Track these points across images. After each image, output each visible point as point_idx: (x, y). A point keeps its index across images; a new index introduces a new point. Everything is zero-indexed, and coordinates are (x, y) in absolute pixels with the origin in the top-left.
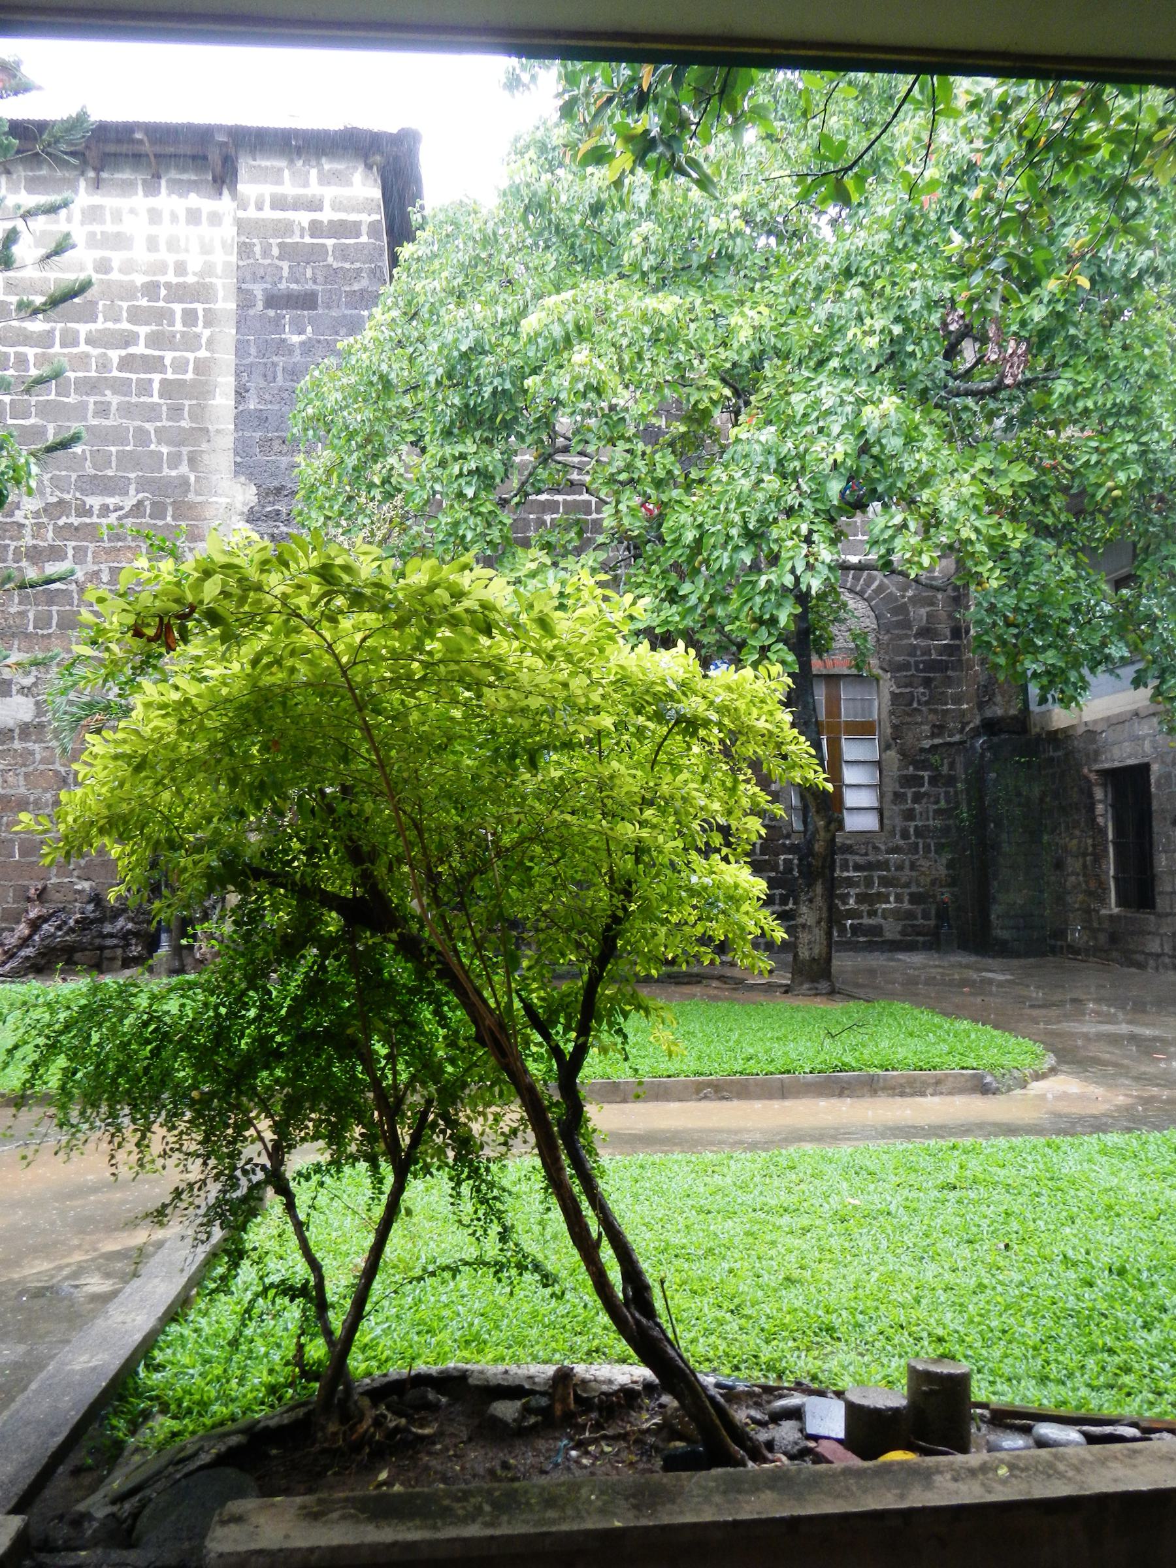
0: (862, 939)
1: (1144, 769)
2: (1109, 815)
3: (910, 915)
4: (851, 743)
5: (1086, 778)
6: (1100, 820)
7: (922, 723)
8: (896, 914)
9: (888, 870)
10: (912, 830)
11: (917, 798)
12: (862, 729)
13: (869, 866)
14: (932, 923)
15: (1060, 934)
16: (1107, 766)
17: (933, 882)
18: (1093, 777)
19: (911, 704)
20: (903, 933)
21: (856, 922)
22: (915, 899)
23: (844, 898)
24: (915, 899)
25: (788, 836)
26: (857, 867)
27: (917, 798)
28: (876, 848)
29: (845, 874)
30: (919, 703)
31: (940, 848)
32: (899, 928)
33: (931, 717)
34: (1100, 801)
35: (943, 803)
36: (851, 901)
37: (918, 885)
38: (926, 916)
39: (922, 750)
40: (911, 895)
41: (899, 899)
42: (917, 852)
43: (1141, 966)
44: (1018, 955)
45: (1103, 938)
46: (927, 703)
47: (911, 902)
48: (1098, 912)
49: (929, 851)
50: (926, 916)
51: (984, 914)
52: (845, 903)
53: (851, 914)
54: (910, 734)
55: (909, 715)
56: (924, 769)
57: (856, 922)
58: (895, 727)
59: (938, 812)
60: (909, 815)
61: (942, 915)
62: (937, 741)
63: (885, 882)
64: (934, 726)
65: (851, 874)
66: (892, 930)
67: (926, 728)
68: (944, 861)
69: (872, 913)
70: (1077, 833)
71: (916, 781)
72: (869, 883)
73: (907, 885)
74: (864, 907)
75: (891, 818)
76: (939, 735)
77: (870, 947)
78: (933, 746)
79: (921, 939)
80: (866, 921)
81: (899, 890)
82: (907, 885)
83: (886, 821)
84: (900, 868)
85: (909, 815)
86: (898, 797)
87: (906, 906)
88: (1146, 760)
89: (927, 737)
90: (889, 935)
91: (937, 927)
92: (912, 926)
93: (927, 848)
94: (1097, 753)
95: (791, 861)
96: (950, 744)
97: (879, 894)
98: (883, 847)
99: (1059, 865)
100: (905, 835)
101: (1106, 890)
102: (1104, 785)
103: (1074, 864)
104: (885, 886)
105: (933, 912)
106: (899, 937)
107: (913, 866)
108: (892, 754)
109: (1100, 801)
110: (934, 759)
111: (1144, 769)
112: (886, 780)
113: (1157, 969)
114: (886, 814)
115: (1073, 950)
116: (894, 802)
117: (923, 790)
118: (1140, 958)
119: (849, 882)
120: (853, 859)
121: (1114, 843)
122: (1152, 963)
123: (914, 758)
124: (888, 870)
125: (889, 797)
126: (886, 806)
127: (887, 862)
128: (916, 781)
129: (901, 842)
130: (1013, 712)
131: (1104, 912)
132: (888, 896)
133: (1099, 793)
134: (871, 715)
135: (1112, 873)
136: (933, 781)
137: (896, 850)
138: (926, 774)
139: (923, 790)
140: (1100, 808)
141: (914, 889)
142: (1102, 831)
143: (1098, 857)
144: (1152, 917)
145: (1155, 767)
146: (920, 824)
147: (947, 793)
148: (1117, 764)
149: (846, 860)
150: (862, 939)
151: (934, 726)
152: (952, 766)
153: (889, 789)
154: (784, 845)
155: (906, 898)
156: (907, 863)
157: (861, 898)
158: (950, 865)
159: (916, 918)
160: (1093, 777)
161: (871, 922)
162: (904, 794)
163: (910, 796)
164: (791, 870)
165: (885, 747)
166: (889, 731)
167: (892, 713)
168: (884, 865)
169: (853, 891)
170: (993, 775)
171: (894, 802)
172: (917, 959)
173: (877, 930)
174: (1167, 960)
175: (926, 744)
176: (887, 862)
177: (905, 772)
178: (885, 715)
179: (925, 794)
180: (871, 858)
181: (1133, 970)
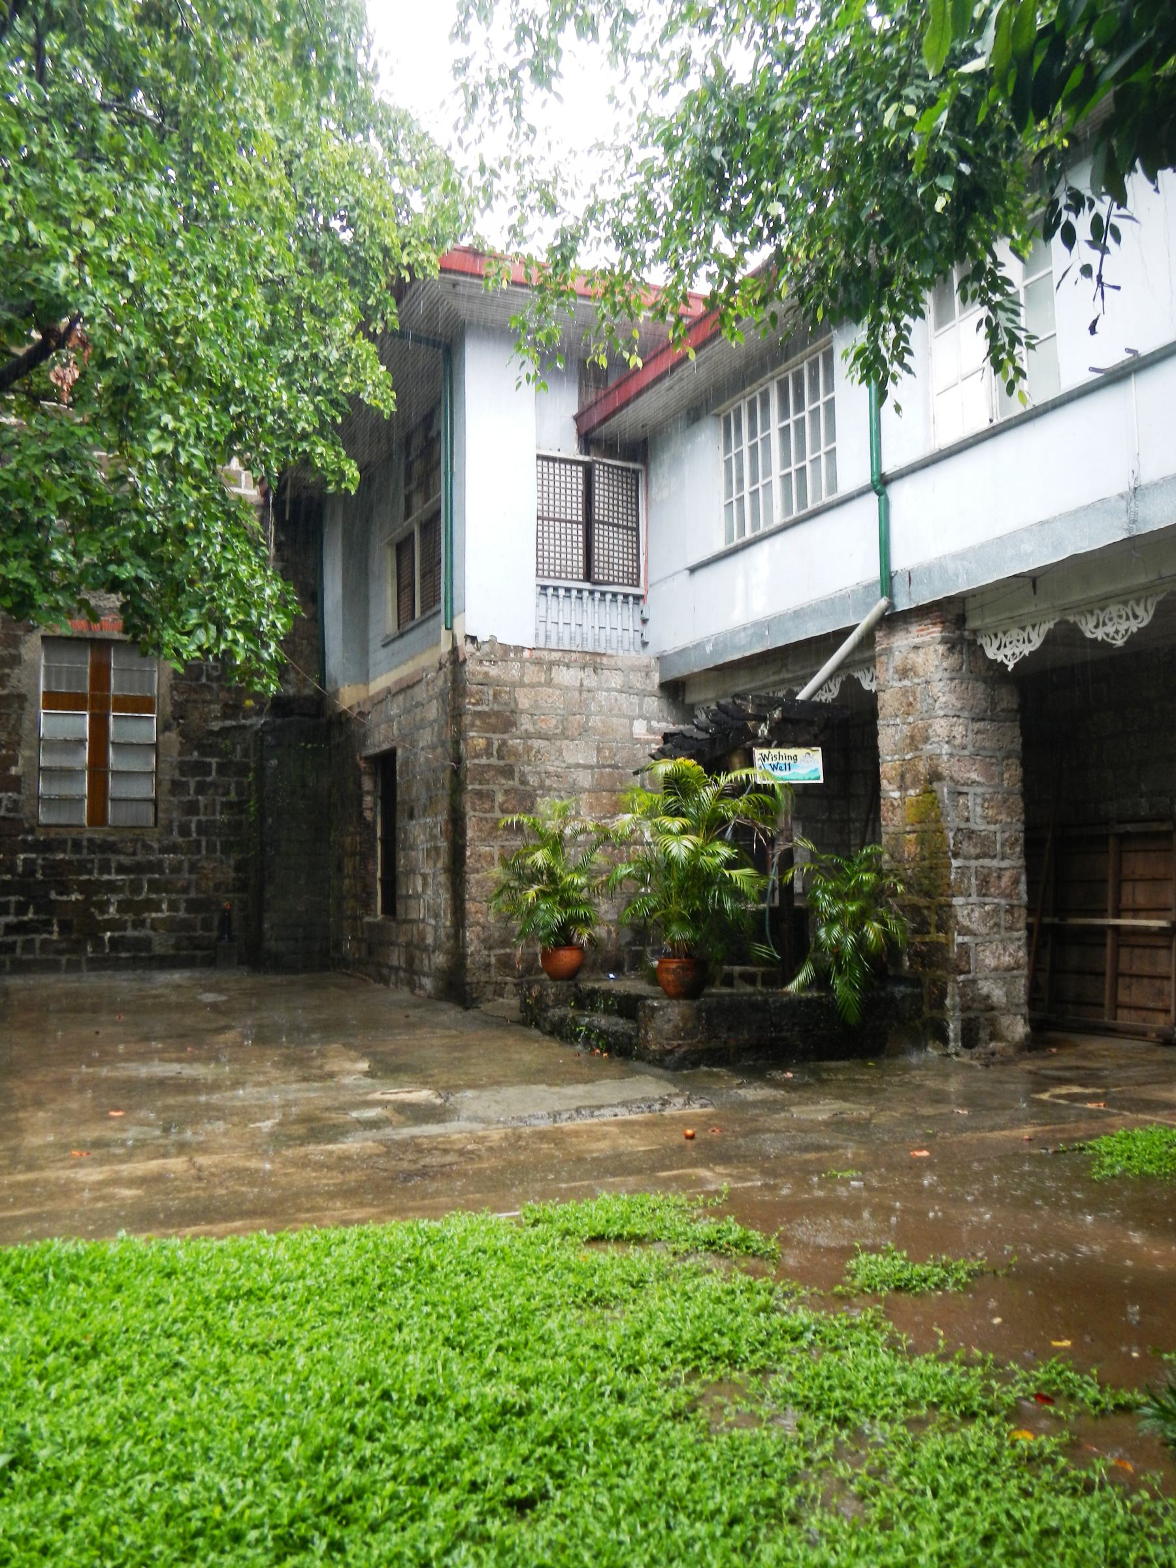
0: (124, 955)
1: (390, 755)
2: (379, 809)
3: (186, 925)
4: (123, 723)
5: (358, 766)
6: (368, 815)
7: (210, 702)
8: (171, 925)
9: (162, 872)
10: (193, 826)
11: (201, 788)
12: (140, 705)
13: (139, 868)
14: (215, 934)
15: (338, 946)
16: (371, 751)
17: (217, 887)
18: (362, 764)
19: (198, 678)
20: (177, 947)
21: (117, 934)
22: (193, 906)
23: (103, 906)
24: (193, 906)
25: (31, 831)
26: (121, 869)
27: (201, 788)
28: (147, 848)
29: (106, 877)
30: (209, 678)
31: (227, 848)
32: (172, 941)
33: (223, 695)
34: (368, 793)
35: (233, 796)
36: (112, 910)
37: (198, 890)
38: (206, 926)
39: (211, 733)
40: (187, 901)
41: (173, 907)
42: (199, 852)
43: (385, 980)
44: (292, 969)
45: (364, 946)
46: (218, 679)
47: (187, 910)
48: (356, 918)
49: (215, 851)
50: (206, 926)
51: (260, 924)
52: (103, 911)
53: (111, 925)
54: (196, 714)
55: (196, 692)
56: (213, 755)
57: (117, 934)
58: (175, 704)
59: (228, 806)
60: (191, 808)
61: (226, 922)
62: (229, 723)
63: (155, 886)
64: (226, 705)
65: (113, 877)
66: (161, 944)
67: (216, 708)
68: (232, 862)
69: (139, 924)
70: (352, 829)
71: (201, 768)
72: (136, 888)
73: (185, 890)
74: (128, 917)
75: (167, 811)
76: (234, 716)
77: (132, 964)
78: (223, 729)
79: (199, 953)
80: (130, 933)
81: (174, 896)
82: (185, 890)
83: (160, 815)
84: (176, 869)
85: (191, 808)
86: (177, 787)
87: (182, 914)
88: (394, 744)
89: (216, 718)
90: (158, 950)
91: (219, 938)
92: (189, 938)
93: (211, 848)
94: (365, 736)
95: (33, 861)
96: (244, 727)
97: (148, 901)
98: (156, 846)
99: (340, 868)
100: (184, 831)
101: (371, 895)
102: (373, 775)
103: (349, 866)
104: (158, 891)
105: (216, 923)
106: (171, 952)
107: (193, 868)
108: (173, 736)
109: (368, 793)
110: (225, 744)
111: (390, 755)
112: (162, 766)
113: (396, 984)
114: (162, 806)
115: (342, 964)
116: (172, 792)
117: (209, 779)
118: (385, 971)
119: (111, 887)
120: (114, 859)
121: (382, 841)
122: (393, 978)
123: (195, 740)
124: (162, 872)
125: (166, 786)
126: (161, 797)
127: (160, 863)
128: (201, 768)
129: (180, 840)
130: (307, 692)
131: (367, 919)
132: (160, 902)
133: (367, 784)
134: (151, 689)
135: (379, 874)
136: (222, 769)
137: (174, 848)
138: (214, 761)
139: (209, 779)
140: (368, 800)
141: (193, 894)
142: (370, 827)
143: (367, 856)
144: (393, 924)
145: (399, 752)
146: (203, 818)
147: (237, 783)
148: (377, 750)
149: (109, 860)
150: (124, 955)
151: (226, 705)
152: (245, 754)
153: (166, 777)
154: (25, 841)
155: (183, 906)
156: (186, 865)
157: (123, 907)
158: (238, 868)
159: (194, 929)
160: (362, 764)
161: (136, 934)
162: (187, 783)
163: (192, 785)
164: (33, 873)
165: (164, 728)
166: (169, 709)
167: (173, 688)
168: (158, 867)
169: (114, 898)
170: (274, 762)
171: (172, 792)
172: (177, 977)
173: (145, 944)
174: (402, 974)
175: (216, 726)
176: (160, 863)
177: (187, 758)
178: (165, 690)
179: (213, 784)
180: (139, 858)
181: (381, 986)
